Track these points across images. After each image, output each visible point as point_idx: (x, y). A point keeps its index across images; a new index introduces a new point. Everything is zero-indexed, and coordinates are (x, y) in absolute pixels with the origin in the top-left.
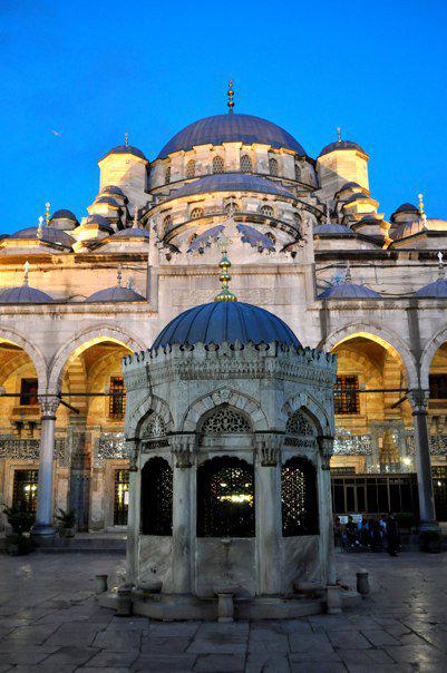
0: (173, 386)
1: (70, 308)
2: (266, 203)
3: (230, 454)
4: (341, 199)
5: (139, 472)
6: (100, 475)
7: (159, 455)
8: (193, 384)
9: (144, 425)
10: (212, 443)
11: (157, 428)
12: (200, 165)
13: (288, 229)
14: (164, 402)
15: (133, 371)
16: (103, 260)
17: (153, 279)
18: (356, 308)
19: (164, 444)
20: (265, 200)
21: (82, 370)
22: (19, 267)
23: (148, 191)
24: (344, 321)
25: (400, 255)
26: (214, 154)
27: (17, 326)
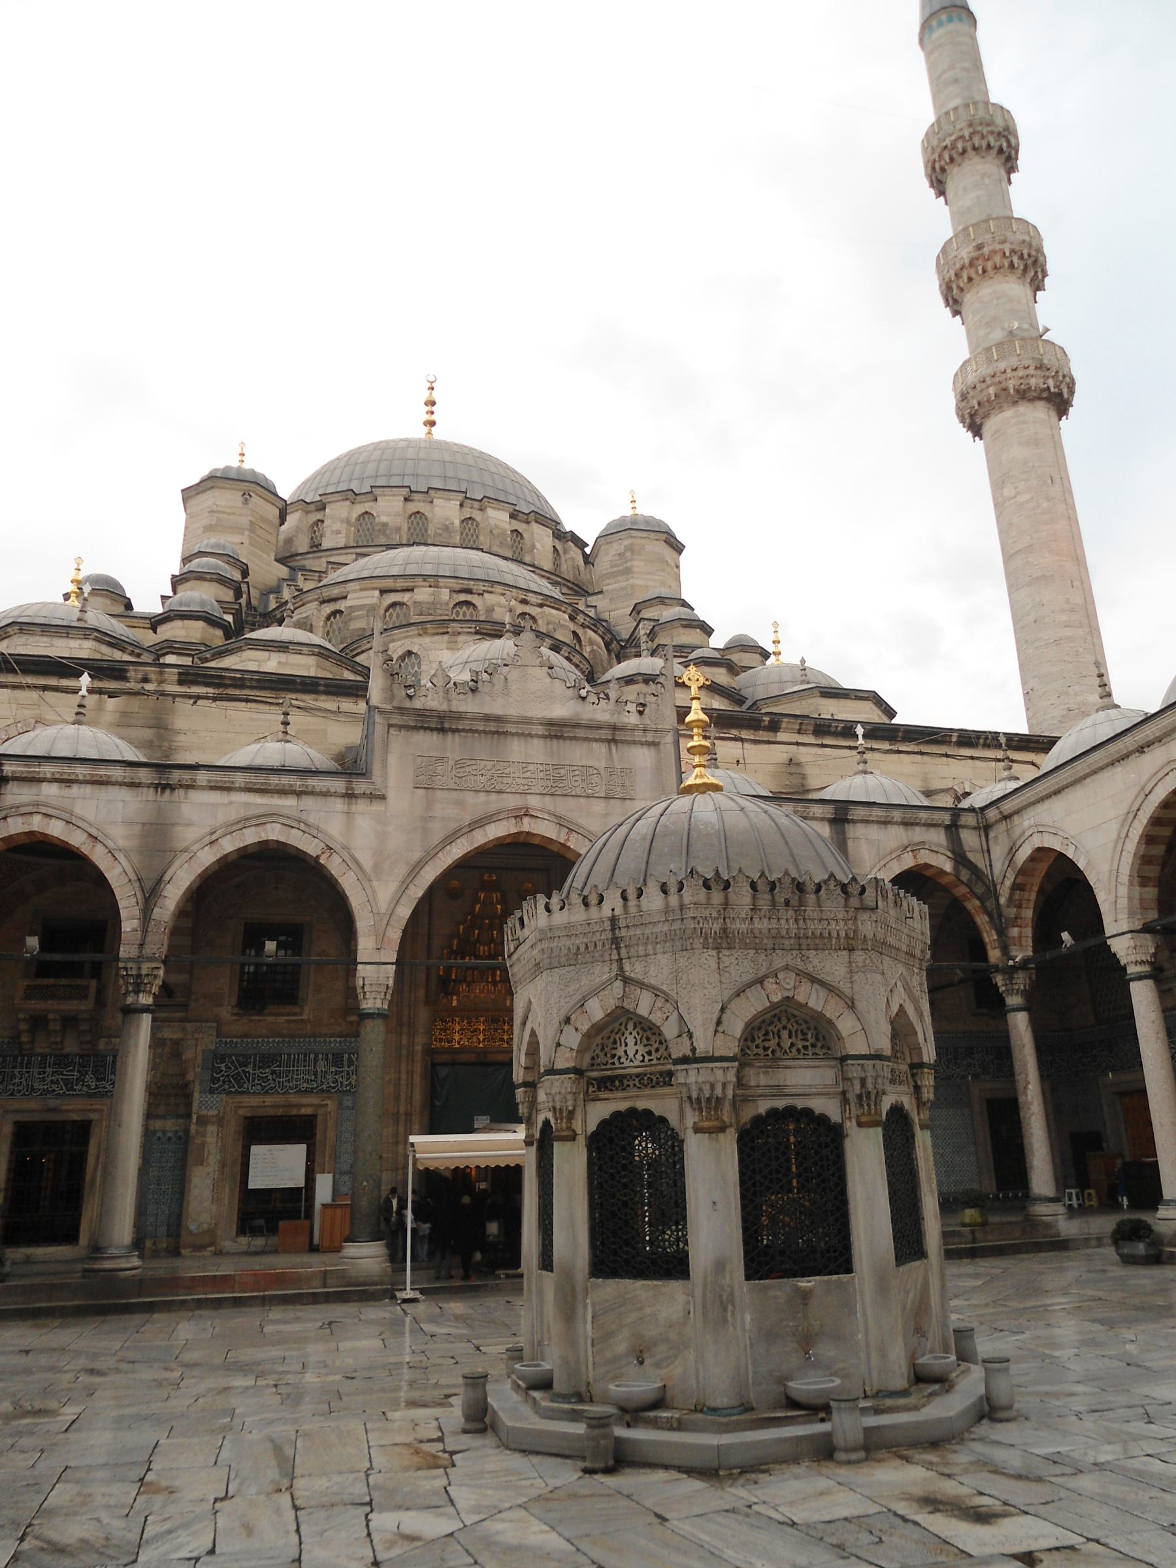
3: (800, 1103)
4: (645, 614)
7: (641, 1105)
8: (728, 958)
10: (763, 1080)
12: (385, 525)
14: (656, 992)
15: (568, 927)
22: (65, 683)
23: (281, 560)
26: (412, 507)
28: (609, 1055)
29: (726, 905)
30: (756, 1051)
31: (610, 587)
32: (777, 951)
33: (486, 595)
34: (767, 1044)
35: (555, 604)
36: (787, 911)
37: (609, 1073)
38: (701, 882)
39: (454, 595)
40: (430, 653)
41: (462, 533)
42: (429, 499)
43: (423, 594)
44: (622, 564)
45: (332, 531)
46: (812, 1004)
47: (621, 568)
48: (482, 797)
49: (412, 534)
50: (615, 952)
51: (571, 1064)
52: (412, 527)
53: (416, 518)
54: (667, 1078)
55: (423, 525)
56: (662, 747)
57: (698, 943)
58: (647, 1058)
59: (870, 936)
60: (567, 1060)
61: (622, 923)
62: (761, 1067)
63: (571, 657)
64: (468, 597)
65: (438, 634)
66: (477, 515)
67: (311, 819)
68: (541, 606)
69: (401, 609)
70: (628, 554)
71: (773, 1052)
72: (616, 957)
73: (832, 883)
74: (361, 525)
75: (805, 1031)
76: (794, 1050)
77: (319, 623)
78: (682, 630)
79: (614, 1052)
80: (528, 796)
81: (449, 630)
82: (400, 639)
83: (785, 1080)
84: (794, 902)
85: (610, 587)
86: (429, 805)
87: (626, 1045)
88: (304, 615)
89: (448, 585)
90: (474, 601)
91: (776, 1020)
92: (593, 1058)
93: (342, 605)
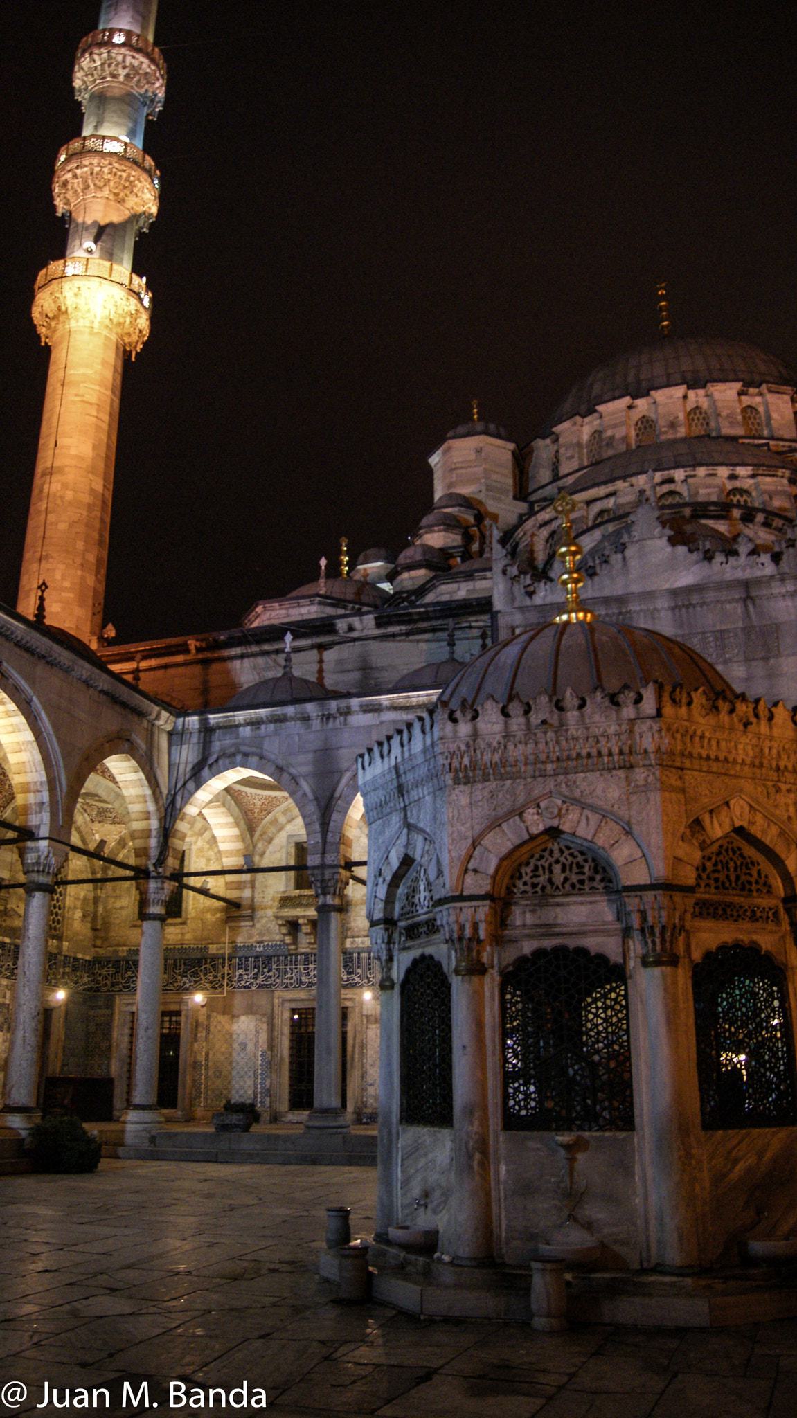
2: (737, 484)
3: (572, 943)
5: (397, 989)
7: (429, 950)
8: (481, 791)
9: (402, 891)
10: (530, 919)
12: (612, 438)
13: (778, 522)
15: (374, 779)
16: (425, 617)
19: (432, 927)
20: (733, 477)
26: (635, 415)
27: (266, 746)
29: (475, 734)
30: (523, 888)
33: (690, 480)
34: (535, 880)
36: (545, 733)
37: (410, 922)
38: (446, 716)
39: (658, 489)
46: (581, 832)
55: (651, 426)
57: (449, 779)
59: (651, 748)
61: (401, 771)
62: (527, 905)
63: (770, 521)
66: (705, 404)
68: (753, 476)
71: (543, 888)
72: (402, 805)
75: (582, 863)
76: (567, 886)
83: (556, 917)
90: (678, 489)
91: (546, 854)
92: (402, 909)
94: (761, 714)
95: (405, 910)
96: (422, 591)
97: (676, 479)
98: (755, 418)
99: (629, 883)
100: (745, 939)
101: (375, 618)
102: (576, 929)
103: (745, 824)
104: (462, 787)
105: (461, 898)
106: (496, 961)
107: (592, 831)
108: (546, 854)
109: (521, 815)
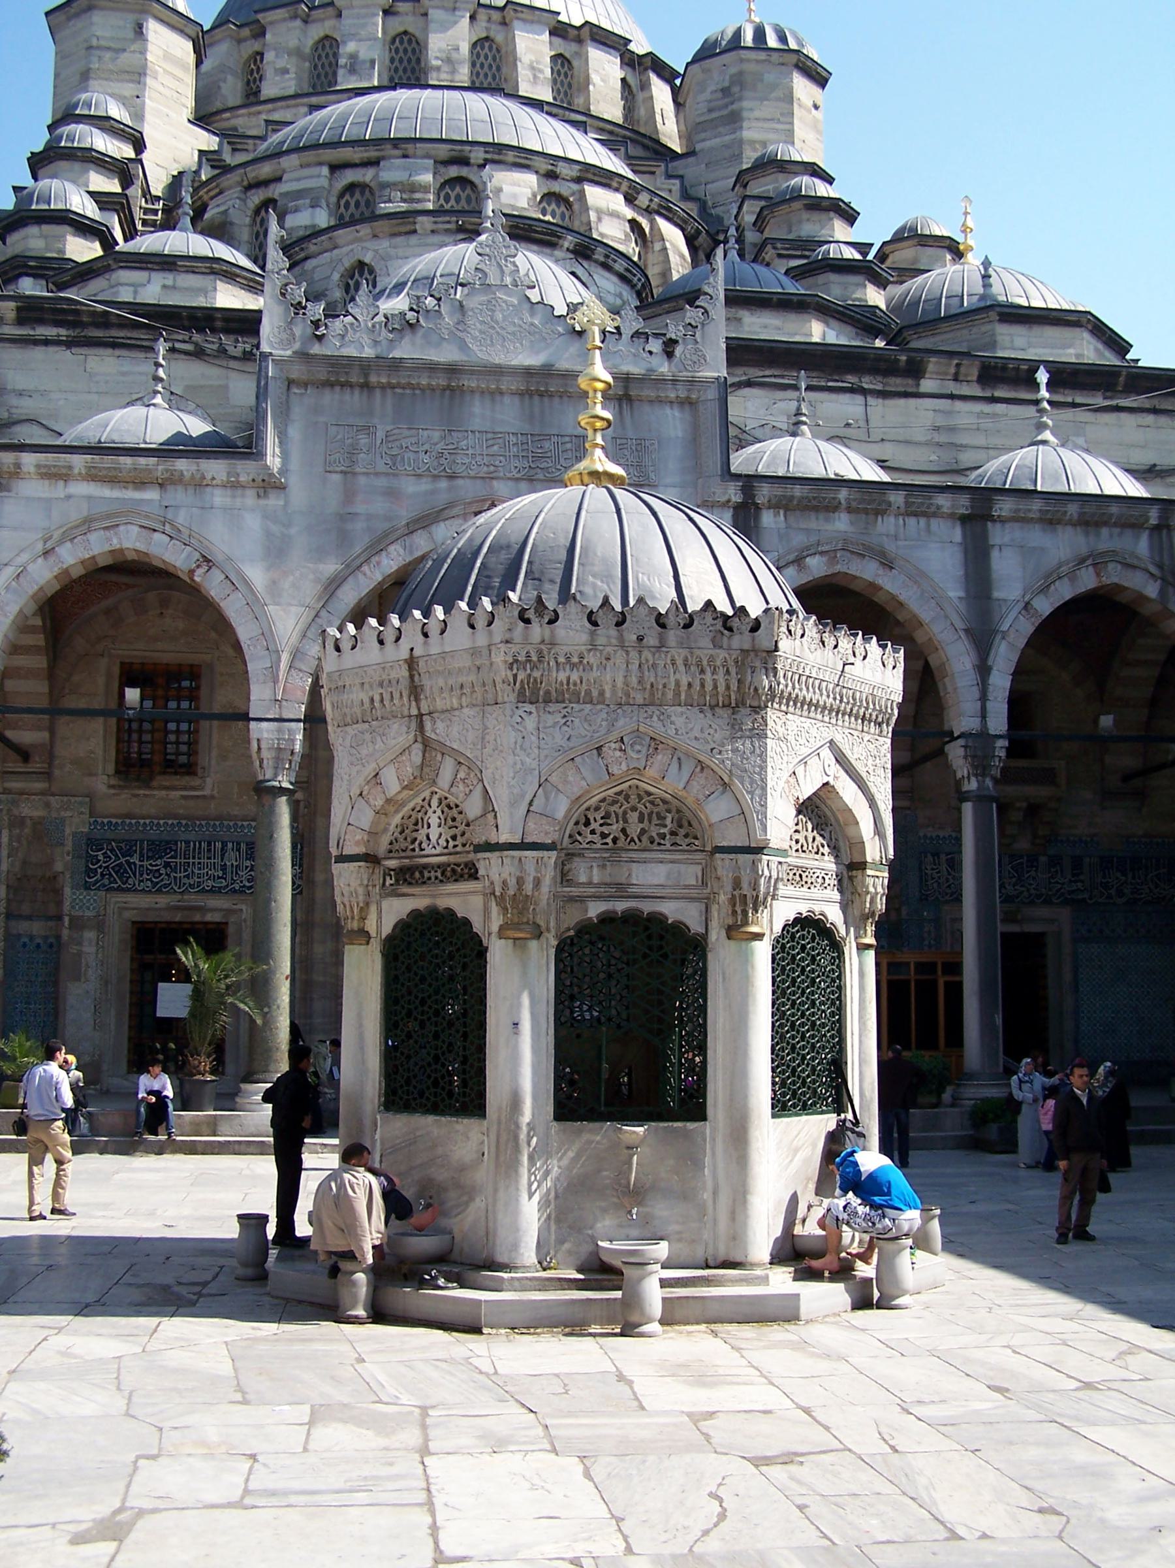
0: (495, 718)
1: (29, 460)
2: (556, 187)
3: (647, 907)
4: (755, 188)
6: (89, 935)
7: (443, 903)
11: (435, 830)
12: (353, 57)
17: (275, 389)
18: (832, 508)
21: (39, 640)
24: (799, 540)
25: (933, 364)
28: (409, 839)
30: (590, 837)
31: (708, 144)
32: (625, 708)
34: (605, 830)
35: (604, 178)
38: (516, 613)
39: (442, 169)
40: (389, 263)
41: (473, 65)
42: (422, 11)
43: (393, 171)
44: (726, 106)
45: (276, 70)
47: (725, 112)
48: (425, 486)
49: (396, 70)
50: (414, 703)
51: (360, 850)
52: (397, 58)
53: (402, 42)
54: (472, 873)
55: (414, 51)
56: (701, 408)
58: (451, 843)
60: (357, 843)
63: (611, 262)
64: (464, 172)
65: (399, 234)
67: (181, 518)
69: (362, 193)
70: (736, 89)
71: (615, 840)
73: (709, 616)
74: (319, 57)
76: (645, 838)
77: (241, 220)
78: (805, 215)
79: (415, 835)
80: (495, 483)
81: (418, 227)
82: (348, 244)
84: (651, 640)
85: (708, 144)
86: (349, 495)
87: (429, 827)
88: (222, 209)
89: (433, 152)
91: (621, 798)
92: (391, 843)
93: (276, 191)
94: (857, 654)
95: (396, 846)
96: (87, 272)
97: (472, 161)
98: (566, 75)
99: (725, 844)
100: (817, 908)
101: (18, 309)
102: (649, 892)
103: (832, 783)
104: (528, 707)
105: (523, 846)
106: (552, 924)
107: (685, 779)
108: (621, 798)
109: (599, 749)
